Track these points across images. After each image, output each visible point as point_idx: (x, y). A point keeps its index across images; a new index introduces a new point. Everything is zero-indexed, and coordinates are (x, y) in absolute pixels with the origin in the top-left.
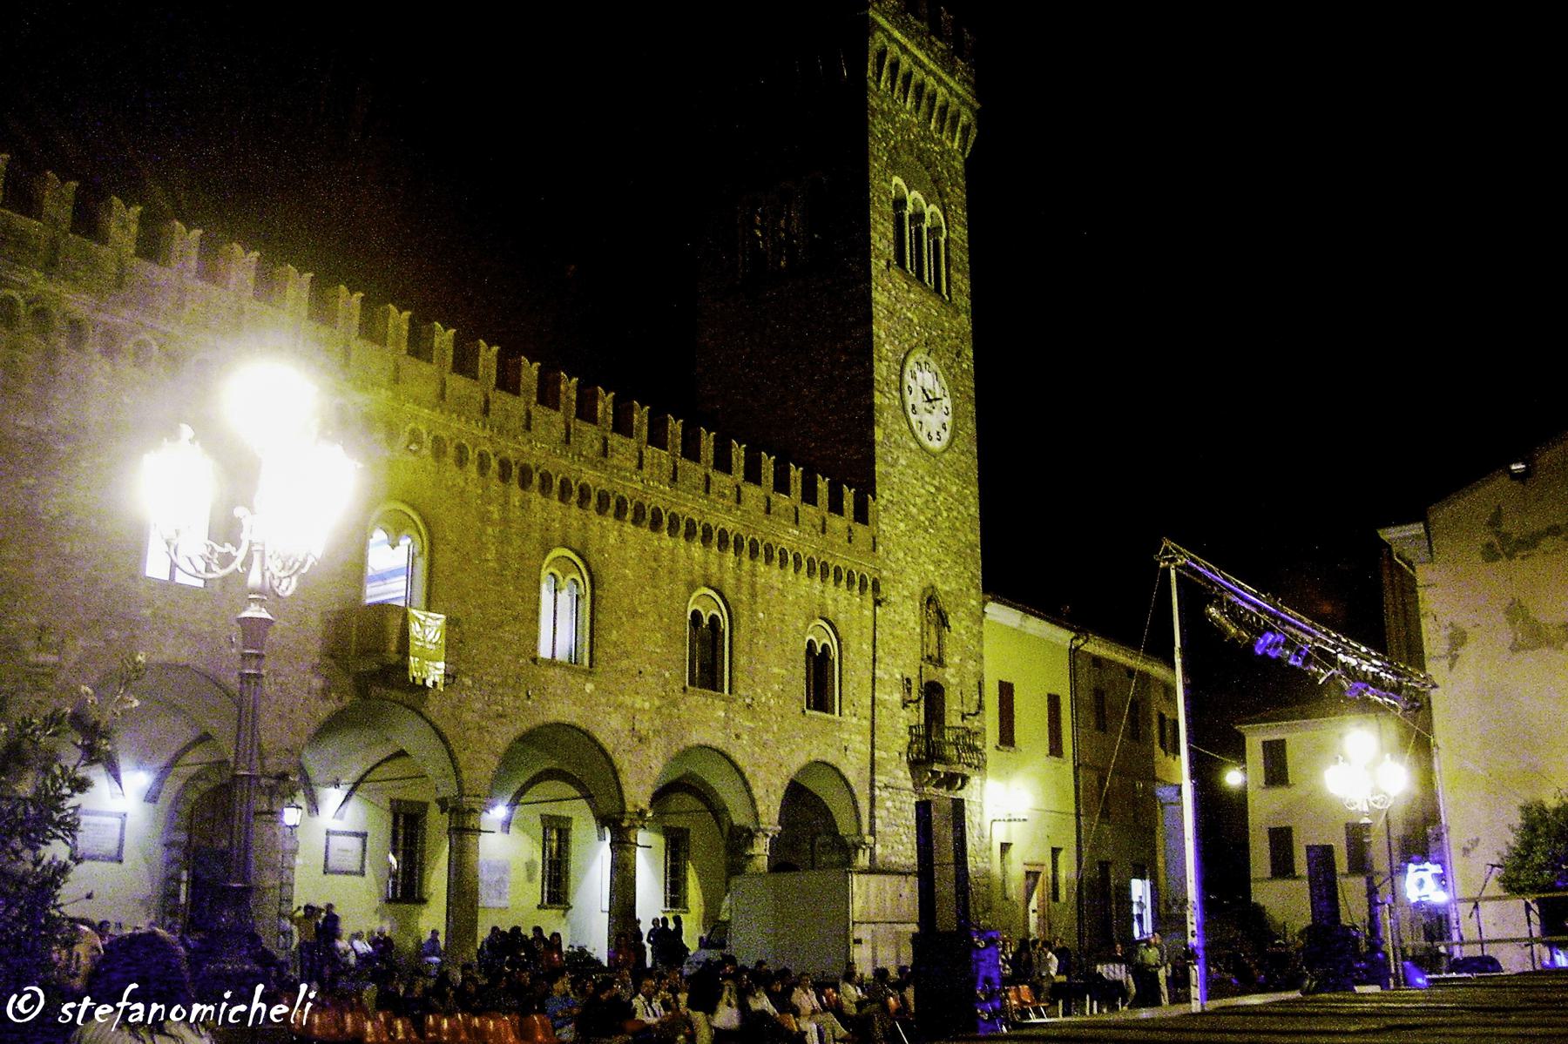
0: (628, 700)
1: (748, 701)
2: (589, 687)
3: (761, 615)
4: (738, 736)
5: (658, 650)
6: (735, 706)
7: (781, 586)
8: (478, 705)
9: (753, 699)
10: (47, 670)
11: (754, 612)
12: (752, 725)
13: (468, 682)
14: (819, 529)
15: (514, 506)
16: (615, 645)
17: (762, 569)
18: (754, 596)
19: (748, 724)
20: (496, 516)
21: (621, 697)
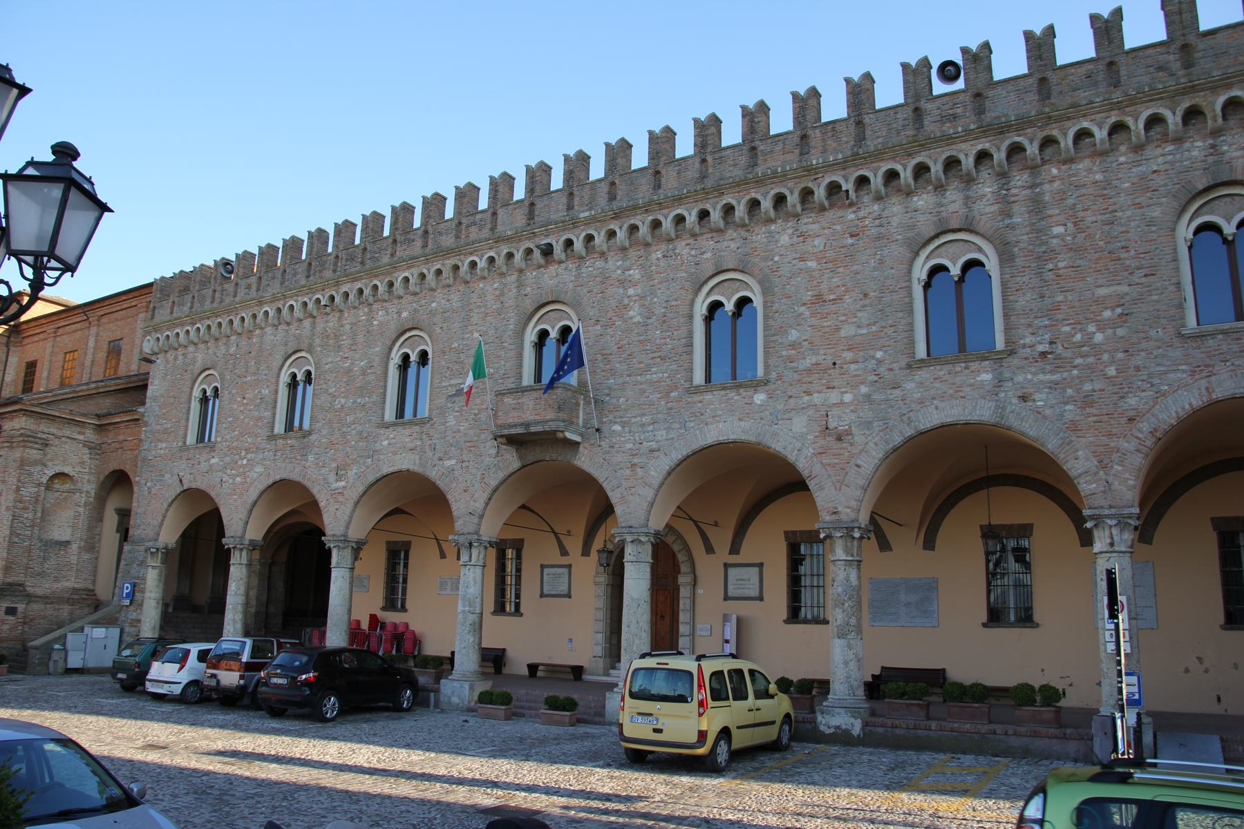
0: (817, 398)
1: (1041, 348)
2: (760, 398)
3: (1058, 230)
4: (1024, 398)
5: (865, 331)
6: (1015, 361)
7: (1099, 177)
8: (629, 446)
9: (1051, 343)
10: (340, 491)
11: (1039, 232)
12: (1055, 377)
13: (617, 428)
14: (1176, 67)
15: (658, 259)
16: (793, 345)
17: (1055, 171)
18: (1037, 206)
19: (1048, 377)
20: (638, 277)
21: (806, 398)
